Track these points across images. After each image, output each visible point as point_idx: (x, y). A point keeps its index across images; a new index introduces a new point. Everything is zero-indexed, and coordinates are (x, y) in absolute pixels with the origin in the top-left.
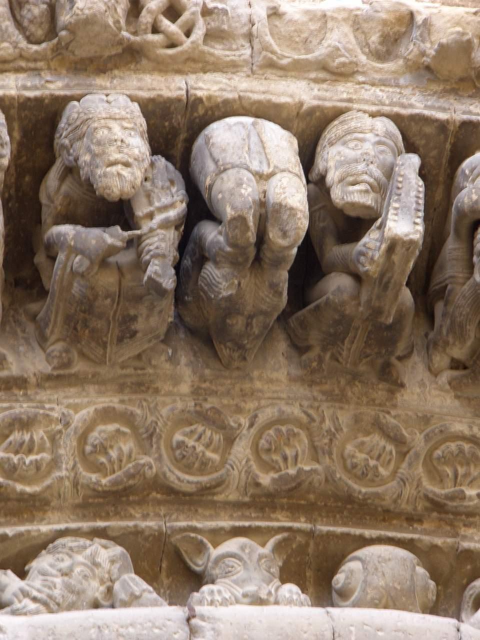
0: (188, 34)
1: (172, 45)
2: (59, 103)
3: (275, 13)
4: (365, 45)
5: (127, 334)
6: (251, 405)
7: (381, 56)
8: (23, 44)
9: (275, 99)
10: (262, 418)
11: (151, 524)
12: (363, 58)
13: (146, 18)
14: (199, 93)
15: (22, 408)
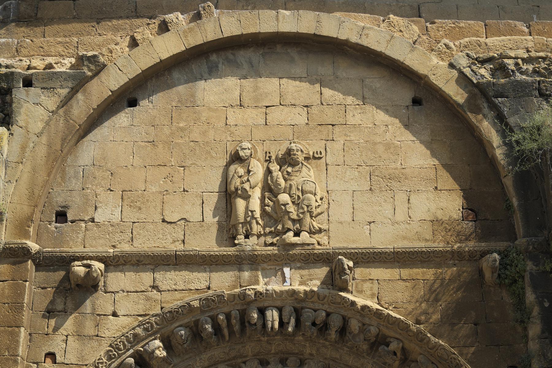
0: (263, 297)
1: (261, 298)
2: (245, 310)
3: (275, 292)
4: (288, 295)
5: (257, 335)
6: (274, 342)
7: (291, 297)
8: (240, 301)
9: (275, 305)
10: (276, 343)
11: (262, 357)
12: (288, 297)
13: (257, 295)
14: (265, 305)
15: (244, 345)
